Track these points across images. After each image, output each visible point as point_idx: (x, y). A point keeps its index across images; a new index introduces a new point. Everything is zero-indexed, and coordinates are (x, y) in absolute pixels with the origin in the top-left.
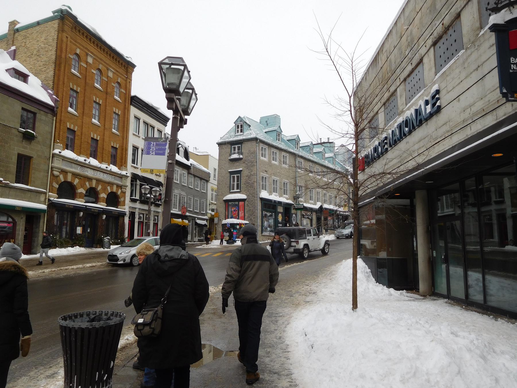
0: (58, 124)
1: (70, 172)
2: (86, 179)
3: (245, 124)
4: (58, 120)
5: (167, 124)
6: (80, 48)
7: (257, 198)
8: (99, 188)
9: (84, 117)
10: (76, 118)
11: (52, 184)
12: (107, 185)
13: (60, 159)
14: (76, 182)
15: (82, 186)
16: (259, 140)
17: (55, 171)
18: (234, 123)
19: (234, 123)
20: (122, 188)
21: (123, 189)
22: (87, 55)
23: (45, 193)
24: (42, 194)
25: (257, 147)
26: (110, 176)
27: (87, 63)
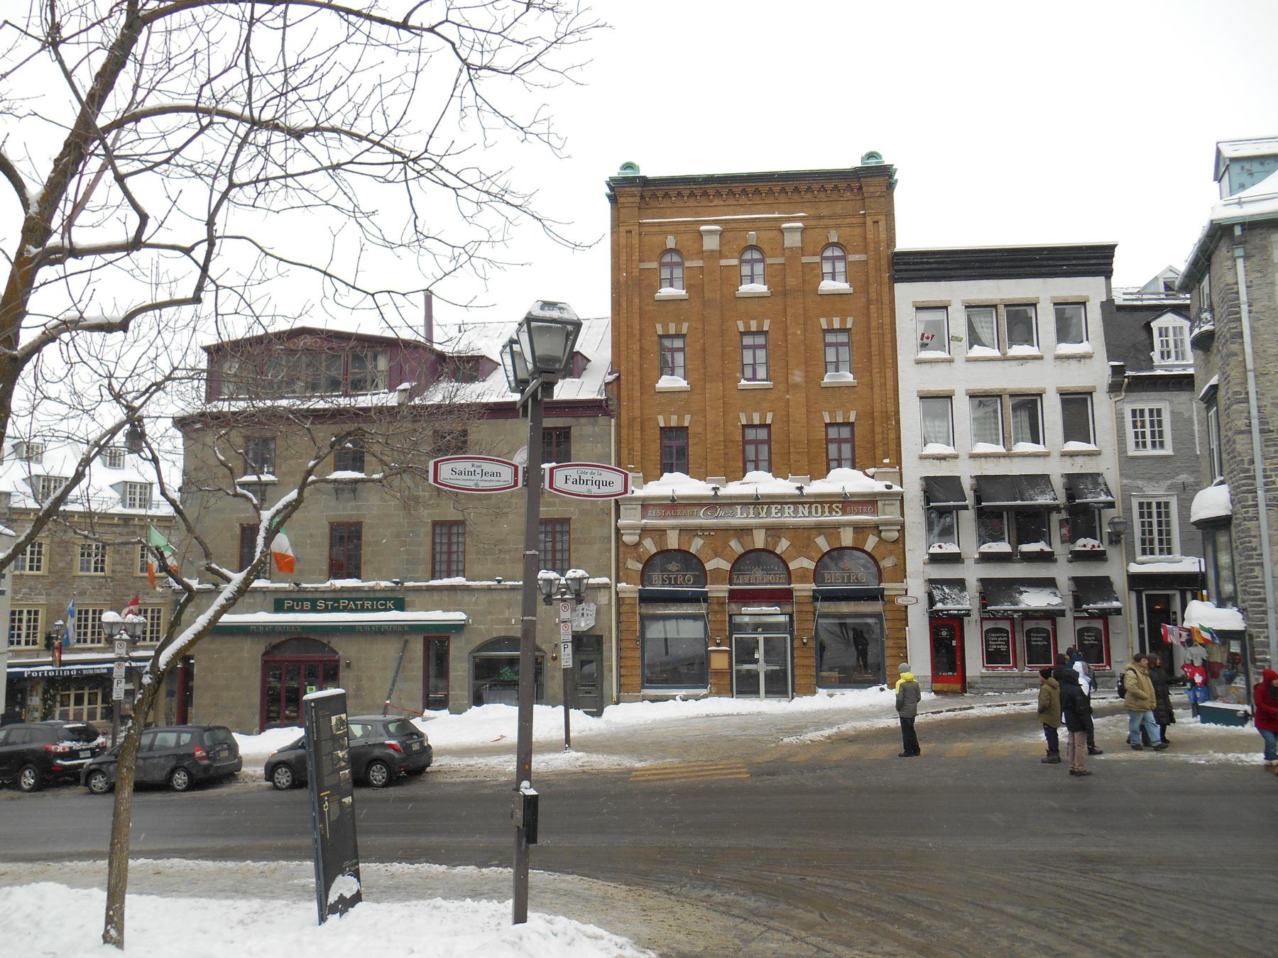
0: (624, 432)
1: (673, 528)
2: (732, 532)
3: (1235, 168)
4: (624, 422)
5: (1114, 266)
6: (671, 233)
7: (1256, 506)
8: (783, 546)
9: (707, 386)
10: (685, 396)
11: (625, 563)
12: (814, 532)
13: (634, 506)
14: (696, 546)
15: (716, 554)
16: (1243, 225)
17: (626, 534)
18: (1215, 180)
19: (1215, 180)
20: (881, 531)
21: (883, 534)
22: (700, 235)
23: (606, 587)
24: (602, 590)
25: (1240, 263)
26: (823, 508)
27: (701, 253)
